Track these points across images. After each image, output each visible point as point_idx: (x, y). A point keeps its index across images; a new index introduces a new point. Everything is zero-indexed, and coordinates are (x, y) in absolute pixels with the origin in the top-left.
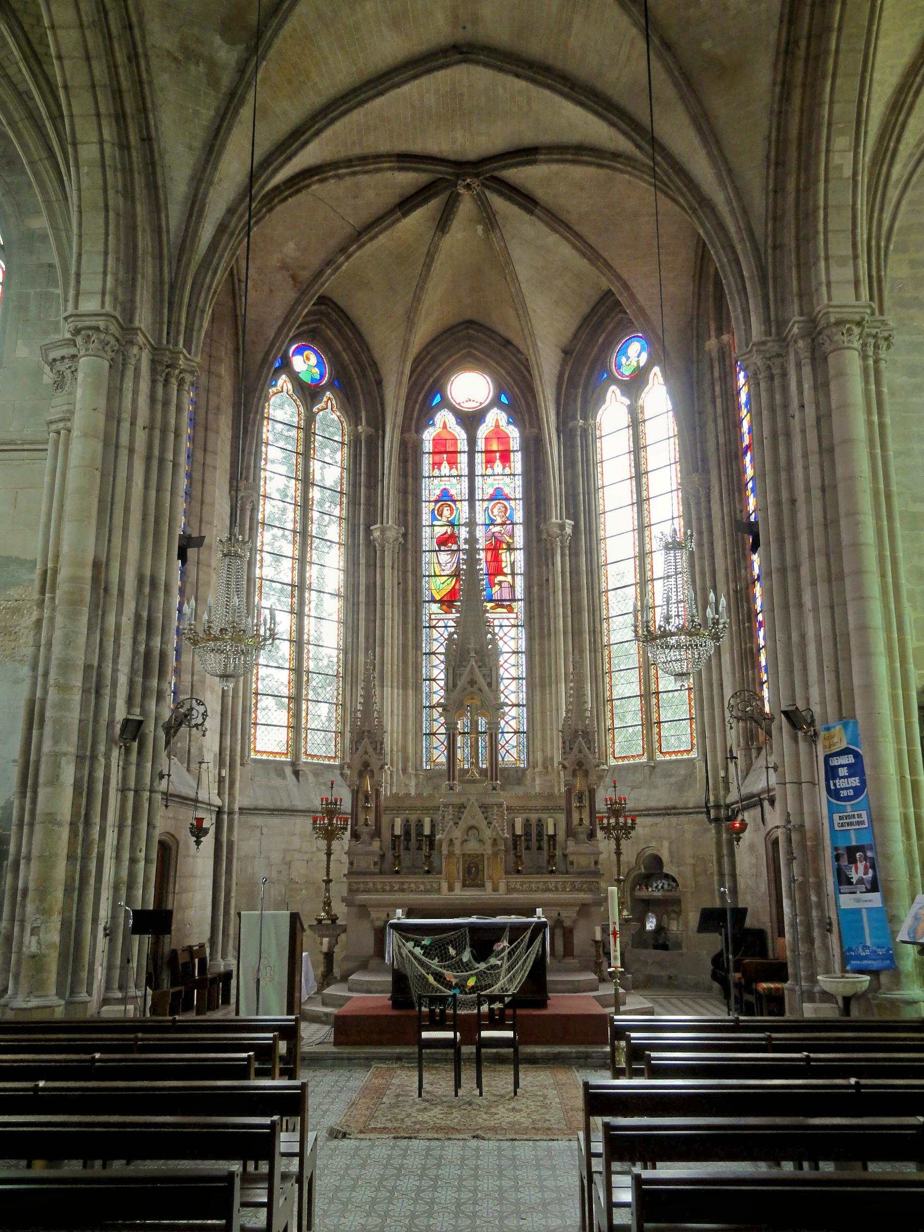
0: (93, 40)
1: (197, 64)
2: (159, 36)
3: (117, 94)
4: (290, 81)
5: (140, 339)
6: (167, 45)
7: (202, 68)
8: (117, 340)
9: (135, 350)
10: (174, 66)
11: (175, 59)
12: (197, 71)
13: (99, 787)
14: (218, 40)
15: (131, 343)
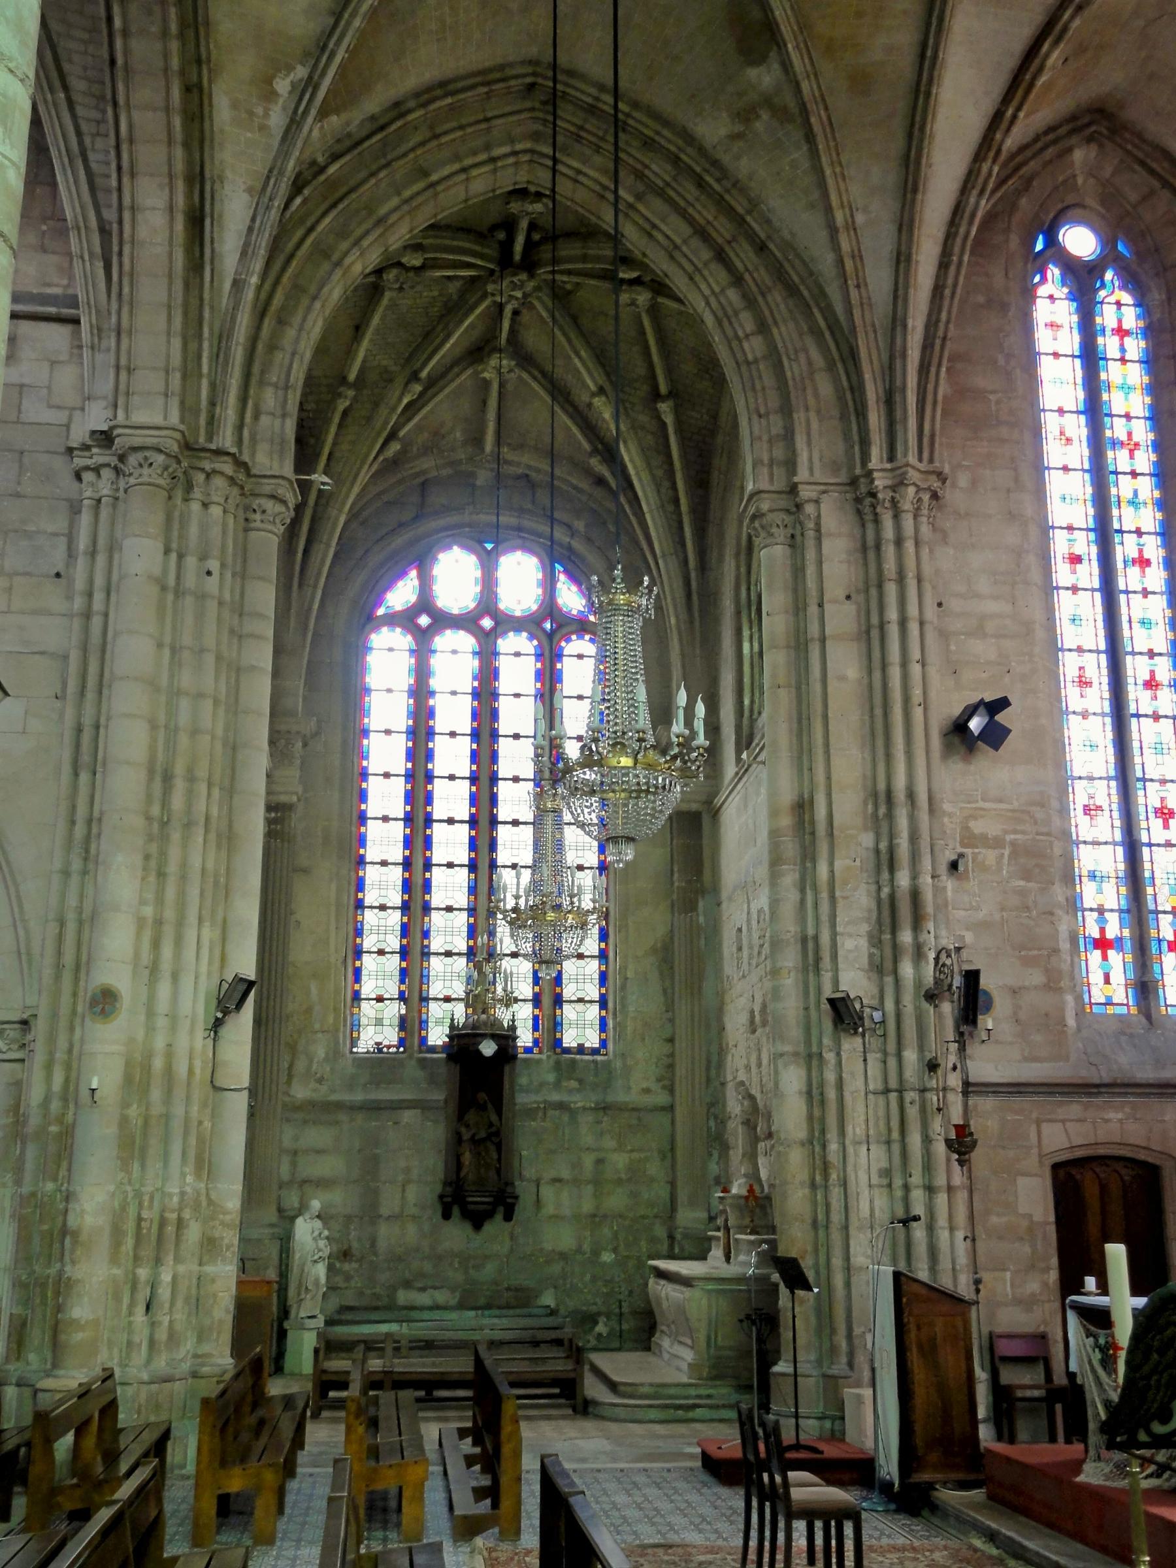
0: (652, 209)
1: (758, 117)
2: (713, 129)
3: (702, 233)
4: (859, 15)
5: (806, 493)
6: (723, 132)
7: (765, 115)
8: (788, 511)
9: (809, 509)
10: (741, 144)
11: (738, 136)
12: (763, 123)
13: (831, 1094)
14: (753, 73)
15: (799, 506)
